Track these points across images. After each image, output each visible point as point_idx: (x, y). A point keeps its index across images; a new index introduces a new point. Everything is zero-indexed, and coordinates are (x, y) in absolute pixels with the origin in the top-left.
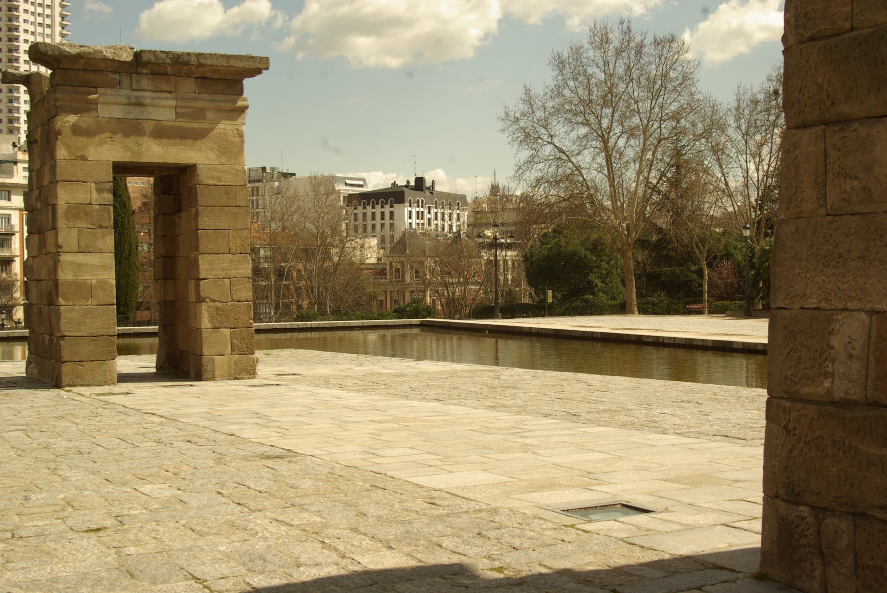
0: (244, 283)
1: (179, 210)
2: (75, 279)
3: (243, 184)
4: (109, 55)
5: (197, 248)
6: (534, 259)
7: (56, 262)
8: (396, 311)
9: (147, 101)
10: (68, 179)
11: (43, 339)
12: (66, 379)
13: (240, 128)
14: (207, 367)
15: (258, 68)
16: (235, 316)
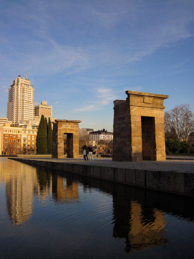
1: (70, 138)
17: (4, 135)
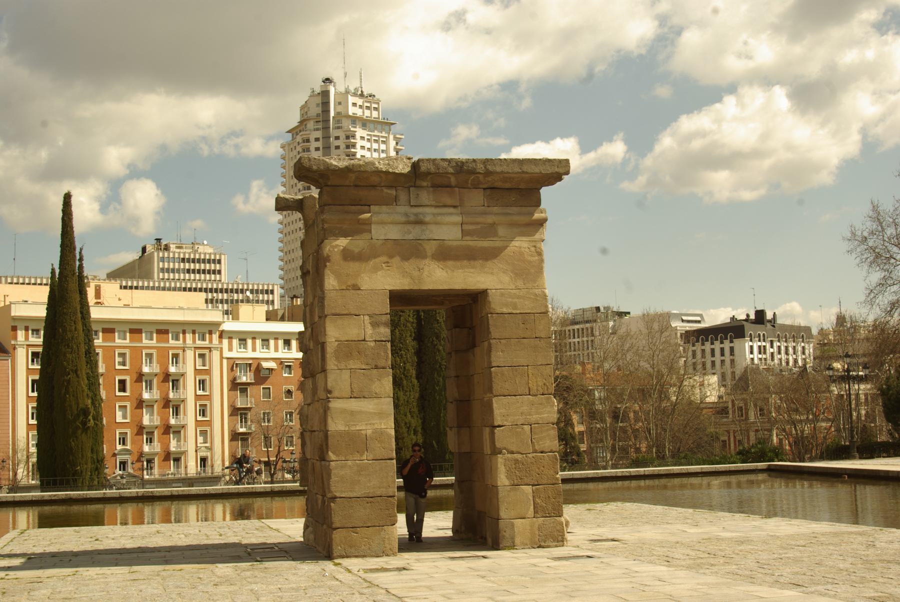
0: (548, 430)
2: (347, 429)
3: (543, 311)
4: (381, 167)
5: (490, 389)
6: (891, 392)
7: (326, 410)
8: (740, 453)
9: (427, 219)
10: (338, 312)
12: (337, 549)
13: (538, 245)
14: (506, 533)
15: (557, 173)
16: (537, 470)
17: (234, 365)
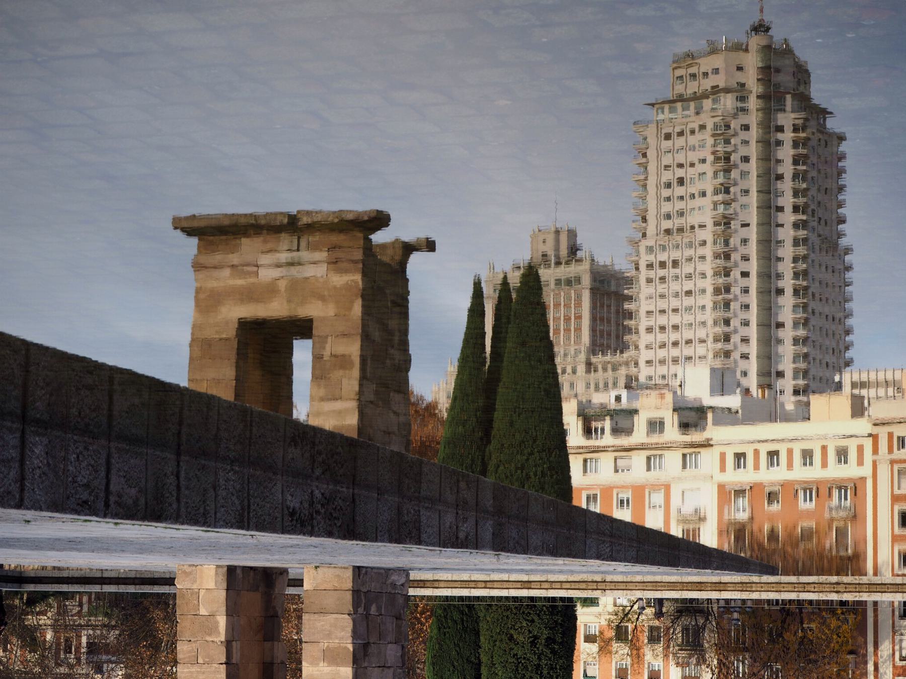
0: (184, 658)
11: (379, 608)
